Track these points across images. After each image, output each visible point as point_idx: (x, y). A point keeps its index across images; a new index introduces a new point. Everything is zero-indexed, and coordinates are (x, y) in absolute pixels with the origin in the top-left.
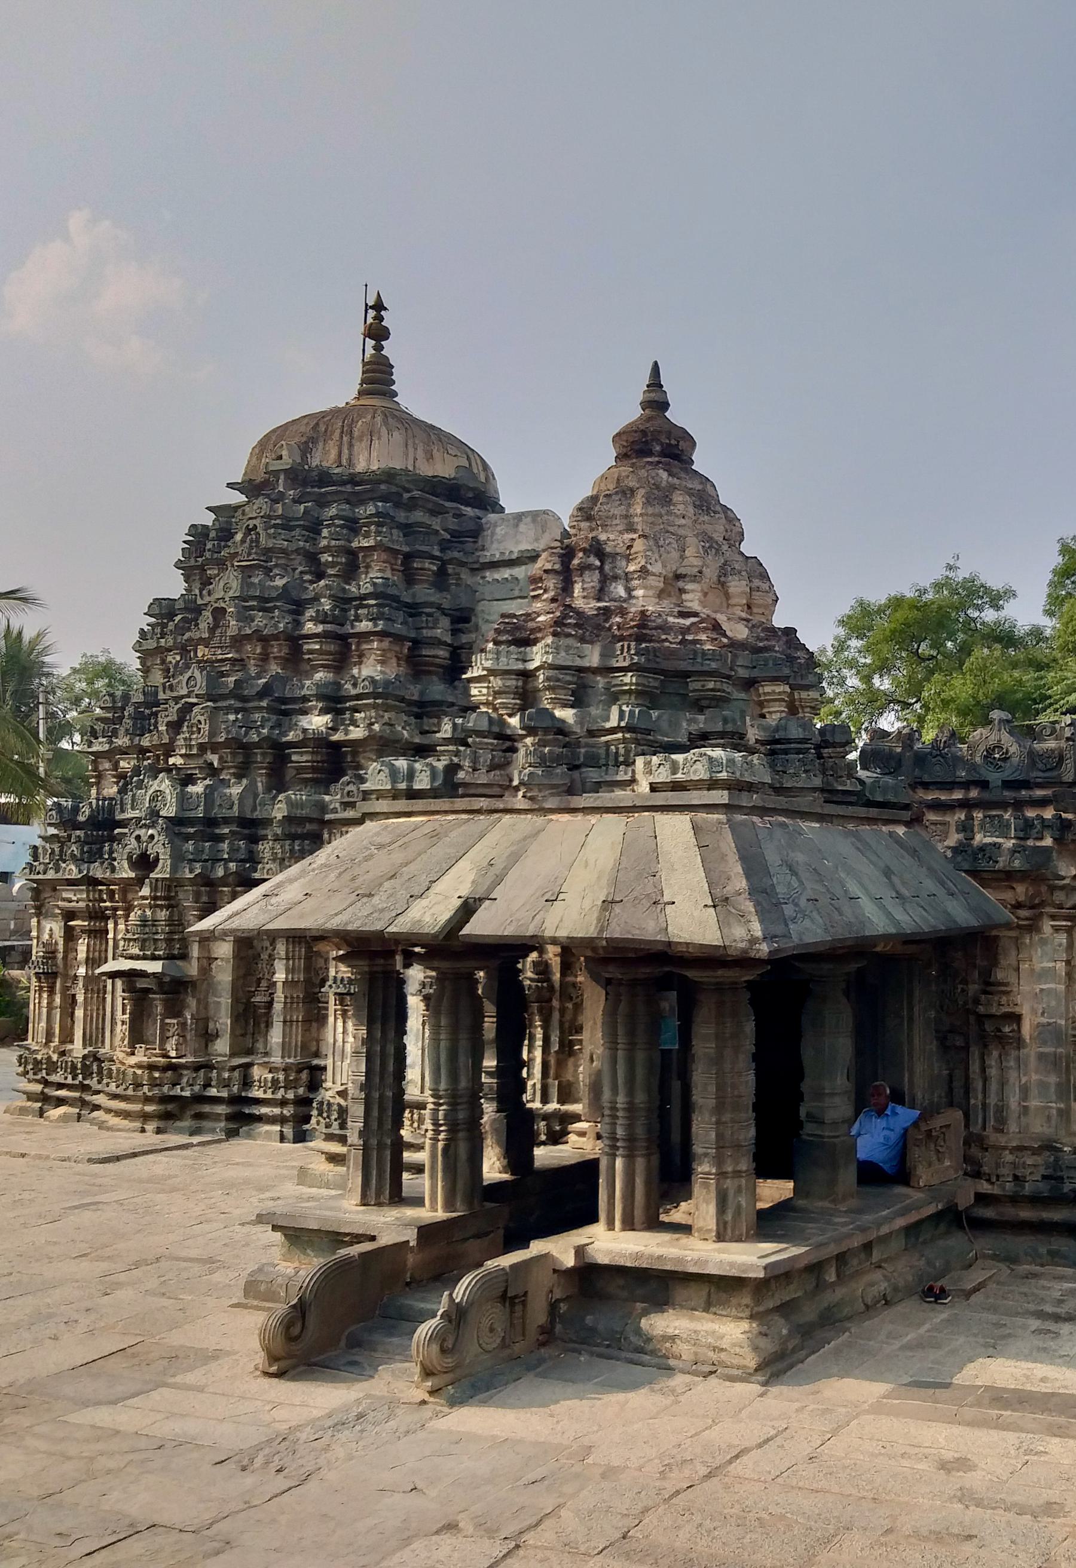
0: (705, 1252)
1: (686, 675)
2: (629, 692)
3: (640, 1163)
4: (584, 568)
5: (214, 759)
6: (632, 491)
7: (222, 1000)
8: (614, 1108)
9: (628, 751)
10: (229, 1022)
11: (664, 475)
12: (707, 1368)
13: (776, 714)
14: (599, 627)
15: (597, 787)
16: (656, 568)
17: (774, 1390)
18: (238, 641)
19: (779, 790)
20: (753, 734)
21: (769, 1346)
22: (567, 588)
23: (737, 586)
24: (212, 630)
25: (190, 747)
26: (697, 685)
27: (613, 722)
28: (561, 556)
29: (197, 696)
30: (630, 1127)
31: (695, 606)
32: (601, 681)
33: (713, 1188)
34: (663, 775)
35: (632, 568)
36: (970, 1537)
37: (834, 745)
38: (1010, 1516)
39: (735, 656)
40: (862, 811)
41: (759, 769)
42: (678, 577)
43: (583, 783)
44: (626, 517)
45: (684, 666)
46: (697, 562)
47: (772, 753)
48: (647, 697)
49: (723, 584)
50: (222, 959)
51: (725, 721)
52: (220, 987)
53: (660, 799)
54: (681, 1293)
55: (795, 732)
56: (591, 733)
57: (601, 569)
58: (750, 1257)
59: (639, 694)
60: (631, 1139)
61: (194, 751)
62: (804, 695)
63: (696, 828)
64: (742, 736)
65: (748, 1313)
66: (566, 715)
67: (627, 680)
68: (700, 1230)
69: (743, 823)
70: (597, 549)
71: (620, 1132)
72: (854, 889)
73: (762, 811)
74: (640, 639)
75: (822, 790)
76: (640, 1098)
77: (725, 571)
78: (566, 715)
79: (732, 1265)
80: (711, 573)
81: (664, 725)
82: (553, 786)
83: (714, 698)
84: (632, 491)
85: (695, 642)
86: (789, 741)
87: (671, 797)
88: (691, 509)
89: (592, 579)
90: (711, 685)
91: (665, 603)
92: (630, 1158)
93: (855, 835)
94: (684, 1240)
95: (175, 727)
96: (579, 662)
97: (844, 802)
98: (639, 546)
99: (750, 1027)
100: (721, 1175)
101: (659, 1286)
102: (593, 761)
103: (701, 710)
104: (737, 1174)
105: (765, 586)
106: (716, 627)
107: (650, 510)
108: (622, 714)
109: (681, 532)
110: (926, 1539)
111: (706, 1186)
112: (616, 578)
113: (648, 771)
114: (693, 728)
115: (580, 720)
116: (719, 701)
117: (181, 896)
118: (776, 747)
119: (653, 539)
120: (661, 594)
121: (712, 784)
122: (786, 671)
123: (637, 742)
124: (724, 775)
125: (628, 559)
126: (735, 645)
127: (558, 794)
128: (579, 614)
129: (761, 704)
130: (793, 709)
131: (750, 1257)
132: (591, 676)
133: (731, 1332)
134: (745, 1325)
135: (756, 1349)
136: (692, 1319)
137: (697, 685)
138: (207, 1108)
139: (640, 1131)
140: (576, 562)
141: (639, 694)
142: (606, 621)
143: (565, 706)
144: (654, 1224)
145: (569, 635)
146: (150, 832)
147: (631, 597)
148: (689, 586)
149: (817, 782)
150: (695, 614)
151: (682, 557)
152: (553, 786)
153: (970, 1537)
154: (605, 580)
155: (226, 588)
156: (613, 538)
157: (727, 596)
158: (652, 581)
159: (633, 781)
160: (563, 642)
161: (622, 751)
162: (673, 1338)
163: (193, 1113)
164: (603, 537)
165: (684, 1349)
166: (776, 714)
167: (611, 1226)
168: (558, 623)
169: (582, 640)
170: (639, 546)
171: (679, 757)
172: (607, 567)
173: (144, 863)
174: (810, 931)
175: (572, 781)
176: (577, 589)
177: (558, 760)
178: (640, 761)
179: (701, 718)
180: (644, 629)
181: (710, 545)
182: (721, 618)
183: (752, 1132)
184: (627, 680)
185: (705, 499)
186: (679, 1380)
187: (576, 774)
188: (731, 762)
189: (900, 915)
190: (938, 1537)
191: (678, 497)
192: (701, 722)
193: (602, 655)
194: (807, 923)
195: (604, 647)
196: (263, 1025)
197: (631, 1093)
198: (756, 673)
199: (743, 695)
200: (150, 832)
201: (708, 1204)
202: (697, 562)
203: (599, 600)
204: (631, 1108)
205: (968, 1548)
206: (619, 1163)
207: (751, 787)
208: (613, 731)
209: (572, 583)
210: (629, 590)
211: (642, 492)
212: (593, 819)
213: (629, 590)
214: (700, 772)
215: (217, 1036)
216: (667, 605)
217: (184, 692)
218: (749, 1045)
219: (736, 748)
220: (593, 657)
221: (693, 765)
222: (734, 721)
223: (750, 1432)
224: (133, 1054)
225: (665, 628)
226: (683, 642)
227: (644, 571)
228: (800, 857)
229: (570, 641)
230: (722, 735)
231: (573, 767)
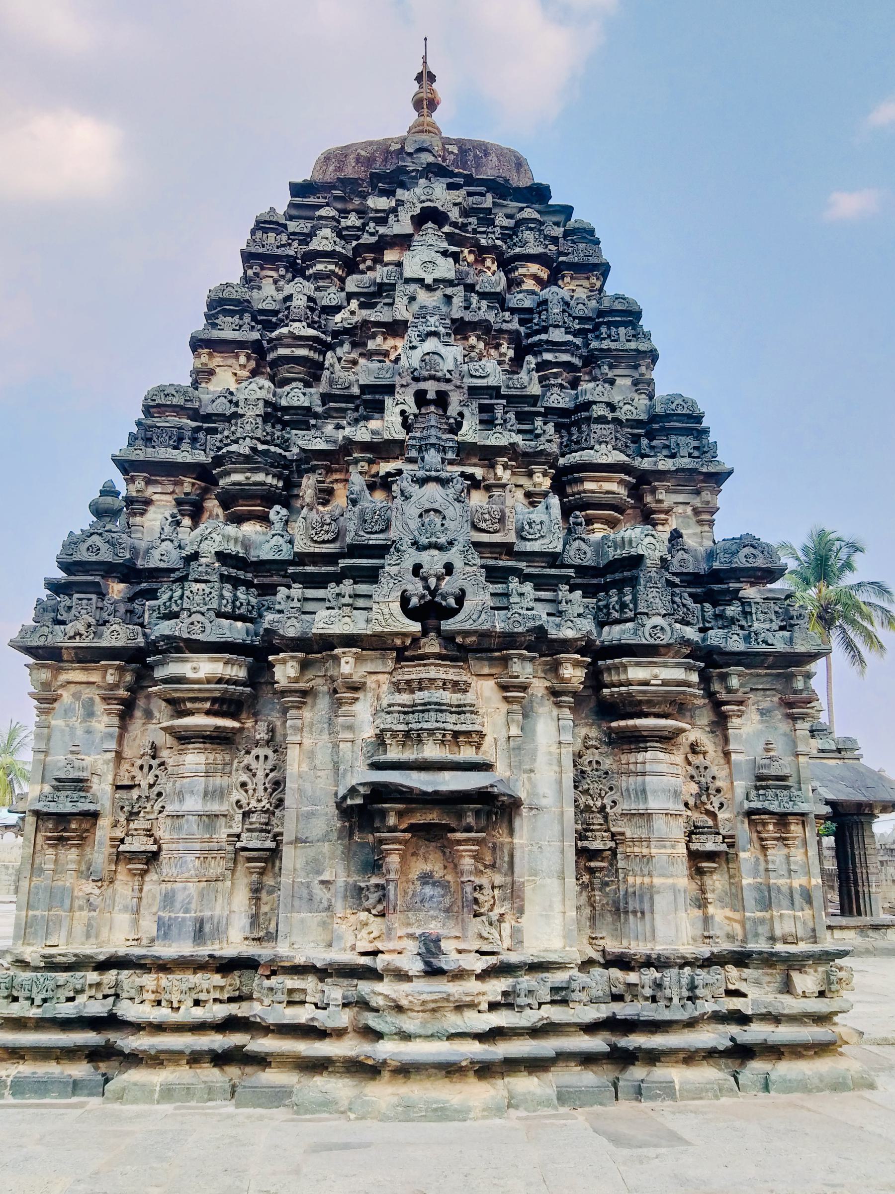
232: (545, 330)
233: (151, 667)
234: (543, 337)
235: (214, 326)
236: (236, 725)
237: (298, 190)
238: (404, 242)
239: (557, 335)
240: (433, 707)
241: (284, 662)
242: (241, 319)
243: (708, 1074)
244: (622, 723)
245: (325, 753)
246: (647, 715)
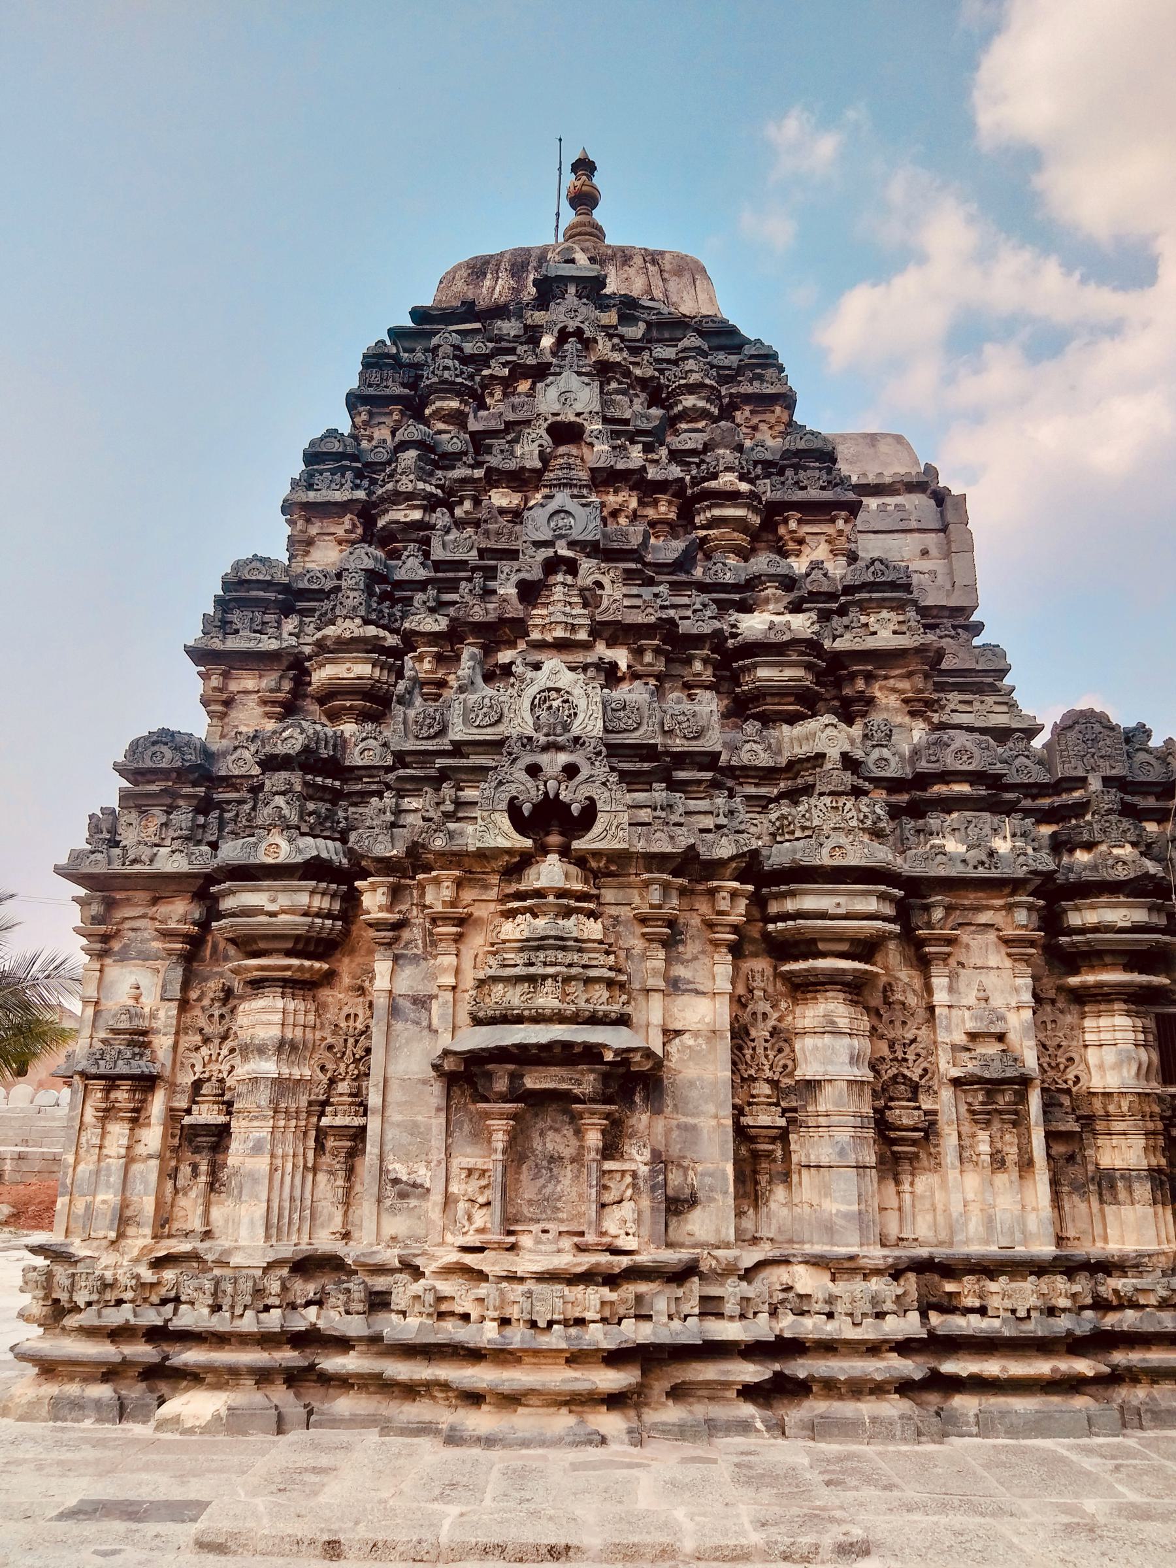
5: (621, 657)
7: (706, 1124)
10: (729, 1169)
18: (605, 479)
24: (544, 458)
25: (574, 628)
29: (572, 545)
50: (696, 1034)
52: (694, 1094)
61: (582, 635)
95: (530, 592)
117: (609, 895)
138: (708, 1371)
146: (563, 758)
155: (565, 397)
163: (667, 1386)
173: (551, 821)
196: (763, 1179)
200: (563, 758)
215: (693, 1201)
217: (545, 535)
224: (513, 1248)
232: (715, 476)
233: (216, 898)
234: (713, 484)
235: (310, 487)
236: (326, 966)
237: (419, 314)
238: (540, 372)
239: (728, 480)
240: (551, 941)
241: (373, 888)
242: (343, 476)
243: (893, 1407)
244: (801, 965)
245: (426, 1000)
246: (823, 955)
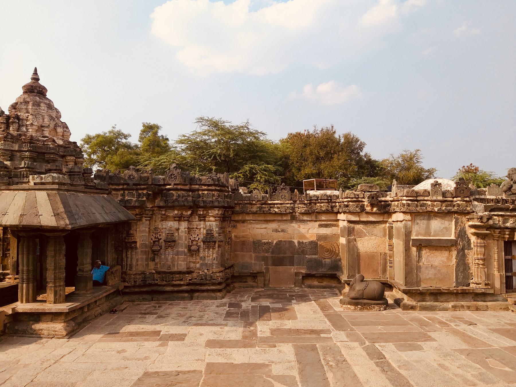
0: (51, 307)
1: (44, 153)
2: (27, 157)
3: (31, 285)
4: (13, 123)
6: (28, 102)
8: (23, 271)
9: (27, 174)
11: (38, 99)
12: (52, 336)
13: (71, 165)
14: (18, 139)
15: (17, 183)
16: (36, 124)
17: (71, 340)
19: (72, 185)
20: (64, 170)
21: (69, 329)
22: (8, 127)
23: (60, 130)
26: (48, 156)
27: (23, 166)
28: (6, 119)
30: (28, 276)
31: (47, 135)
32: (18, 154)
33: (53, 290)
34: (38, 181)
35: (28, 123)
36: (126, 368)
37: (87, 173)
38: (136, 361)
39: (59, 149)
40: (95, 191)
41: (66, 179)
42: (42, 126)
43: (13, 182)
44: (26, 109)
45: (43, 151)
46: (48, 123)
47: (70, 175)
48: (33, 159)
49: (55, 129)
51: (57, 166)
53: (37, 187)
54: (44, 318)
55: (77, 170)
56: (15, 168)
57: (18, 123)
58: (64, 307)
59: (30, 158)
60: (28, 279)
62: (79, 160)
63: (48, 195)
64: (61, 170)
65: (63, 321)
66: (8, 163)
67: (27, 154)
68: (49, 301)
69: (62, 194)
70: (17, 117)
71: (25, 277)
72: (94, 211)
73: (68, 191)
74: (30, 143)
75: (84, 185)
76: (31, 268)
77: (56, 126)
78: (8, 163)
79: (59, 309)
80: (52, 126)
81: (38, 167)
82: (3, 183)
83: (52, 160)
84: (28, 102)
85: (47, 145)
86: (75, 172)
87: (40, 186)
88: (46, 108)
89: (16, 126)
90: (52, 156)
91: (38, 133)
92: (28, 284)
93: (94, 197)
94: (44, 304)
96: (12, 149)
97: (90, 188)
98: (30, 117)
99: (64, 247)
100: (55, 286)
101: (37, 317)
102: (16, 176)
103: (49, 163)
104: (60, 286)
105: (68, 130)
106: (54, 141)
107: (34, 108)
108: (25, 163)
109: (43, 114)
110: (115, 370)
111: (51, 290)
112: (23, 126)
113: (33, 179)
114: (47, 168)
115: (12, 165)
116: (54, 161)
118: (71, 173)
119: (35, 116)
120: (37, 131)
121: (53, 183)
122: (74, 153)
123: (30, 171)
124: (57, 181)
125: (27, 121)
126: (59, 146)
127: (5, 185)
128: (12, 135)
129: (67, 162)
130: (76, 163)
131: (64, 307)
132: (15, 153)
133: (59, 326)
134: (63, 324)
135: (66, 330)
136: (47, 324)
137: (48, 156)
139: (31, 276)
140: (11, 121)
141: (30, 158)
142: (20, 137)
143: (7, 161)
144: (35, 300)
145: (8, 141)
147: (27, 131)
148: (46, 129)
149: (83, 183)
150: (47, 137)
151: (43, 121)
152: (3, 183)
153: (126, 368)
154: (20, 126)
156: (22, 115)
157: (57, 132)
158: (34, 127)
159: (29, 182)
160: (7, 143)
161: (25, 174)
162: (42, 330)
164: (19, 114)
165: (45, 332)
166: (71, 165)
167: (22, 302)
168: (5, 137)
169: (13, 142)
170: (30, 117)
171: (43, 176)
172: (20, 123)
174: (82, 222)
175: (10, 182)
176: (11, 128)
177: (5, 176)
178: (31, 177)
179: (49, 165)
180: (32, 140)
181: (52, 118)
182: (55, 138)
183: (65, 275)
184: (27, 154)
185: (50, 106)
186: (44, 340)
187: (11, 180)
188: (59, 177)
189: (106, 218)
190: (118, 369)
191: (42, 105)
192: (49, 166)
193: (19, 147)
194: (82, 220)
195: (19, 145)
197: (28, 266)
198: (65, 154)
199: (61, 159)
201: (51, 294)
202: (48, 123)
203: (18, 131)
204: (28, 271)
205: (126, 370)
206: (24, 285)
207: (64, 184)
208: (22, 168)
209: (10, 126)
210: (27, 129)
211: (31, 103)
212: (16, 192)
213: (27, 129)
214: (50, 180)
216: (38, 134)
218: (64, 252)
219: (59, 173)
220: (16, 147)
221: (47, 178)
222: (59, 166)
223: (65, 351)
225: (39, 140)
226: (44, 144)
227: (32, 124)
228: (79, 203)
229: (9, 142)
230: (55, 170)
231: (10, 178)
